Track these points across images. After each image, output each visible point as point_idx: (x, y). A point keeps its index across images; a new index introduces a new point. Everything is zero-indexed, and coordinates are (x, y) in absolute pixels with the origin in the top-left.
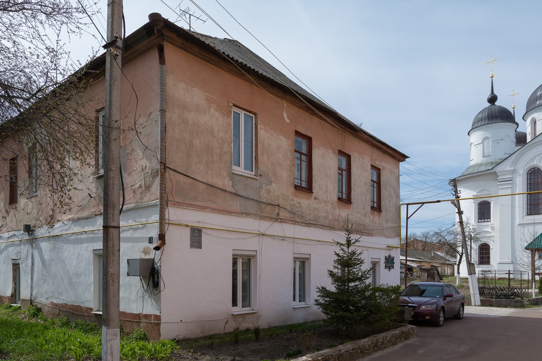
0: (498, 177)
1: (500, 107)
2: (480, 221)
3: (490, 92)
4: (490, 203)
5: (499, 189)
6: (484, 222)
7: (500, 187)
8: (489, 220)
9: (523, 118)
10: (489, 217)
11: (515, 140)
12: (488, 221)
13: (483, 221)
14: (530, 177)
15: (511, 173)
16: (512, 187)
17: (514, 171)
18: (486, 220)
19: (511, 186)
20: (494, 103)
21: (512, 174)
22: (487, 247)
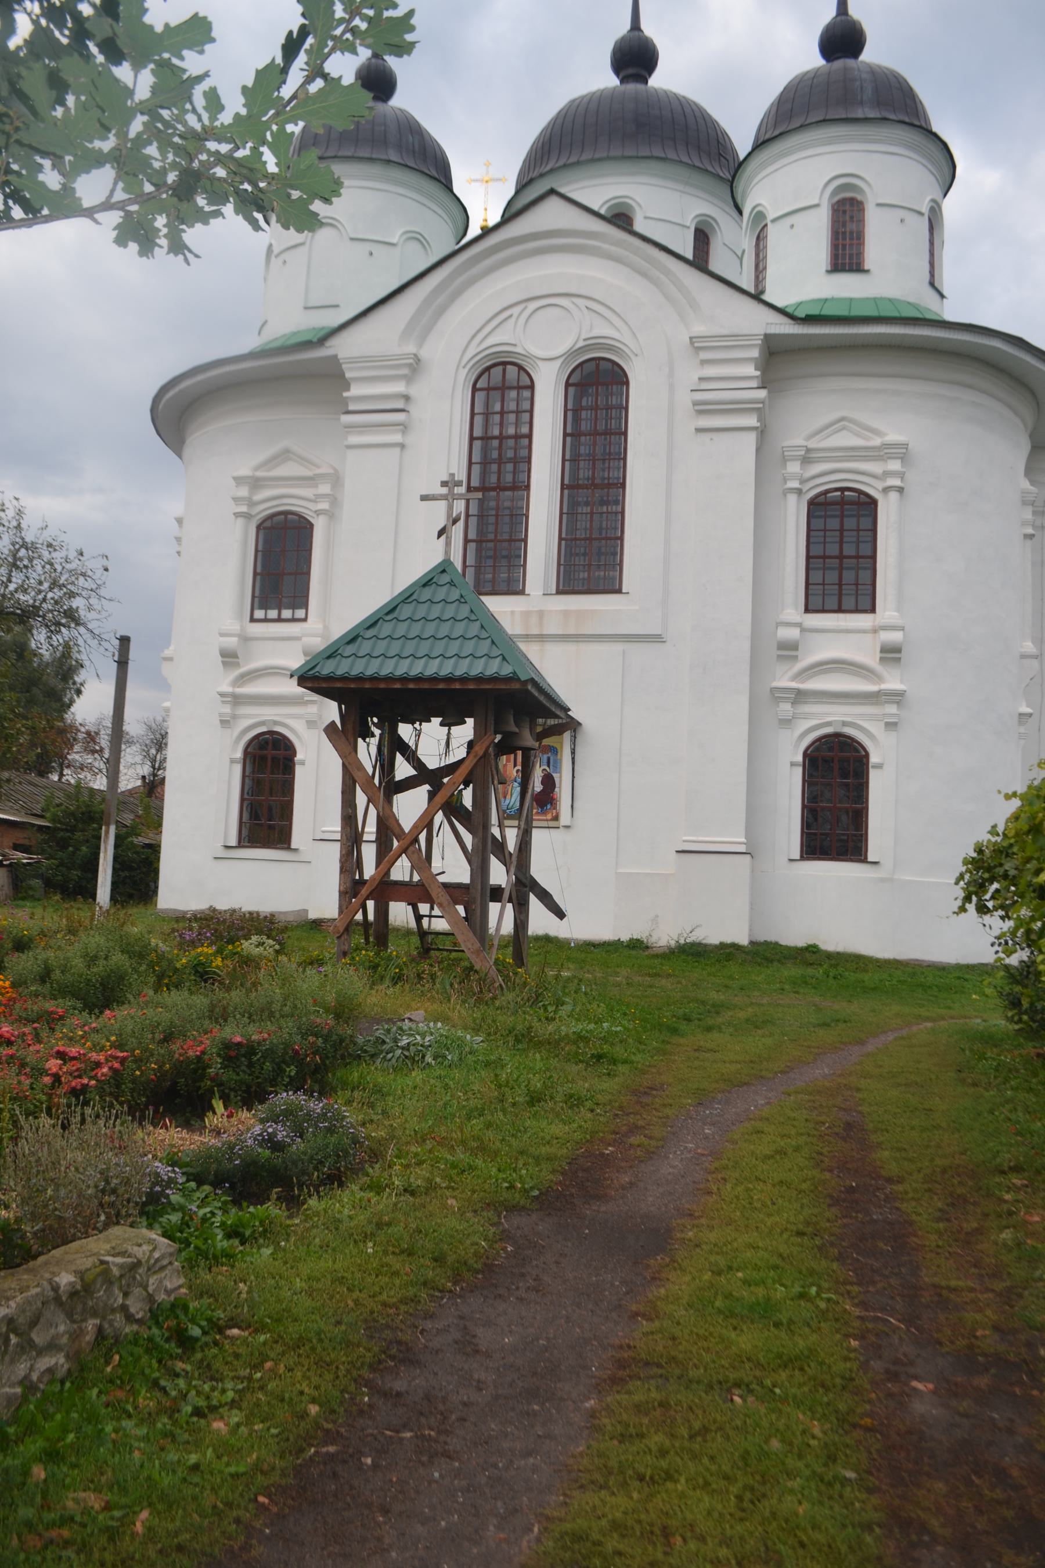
0: (346, 385)
2: (259, 614)
4: (311, 526)
5: (350, 447)
6: (279, 620)
7: (354, 439)
8: (300, 613)
10: (300, 599)
12: (294, 620)
13: (273, 614)
15: (405, 371)
16: (402, 446)
17: (415, 367)
18: (287, 613)
19: (397, 438)
21: (409, 379)
22: (280, 753)
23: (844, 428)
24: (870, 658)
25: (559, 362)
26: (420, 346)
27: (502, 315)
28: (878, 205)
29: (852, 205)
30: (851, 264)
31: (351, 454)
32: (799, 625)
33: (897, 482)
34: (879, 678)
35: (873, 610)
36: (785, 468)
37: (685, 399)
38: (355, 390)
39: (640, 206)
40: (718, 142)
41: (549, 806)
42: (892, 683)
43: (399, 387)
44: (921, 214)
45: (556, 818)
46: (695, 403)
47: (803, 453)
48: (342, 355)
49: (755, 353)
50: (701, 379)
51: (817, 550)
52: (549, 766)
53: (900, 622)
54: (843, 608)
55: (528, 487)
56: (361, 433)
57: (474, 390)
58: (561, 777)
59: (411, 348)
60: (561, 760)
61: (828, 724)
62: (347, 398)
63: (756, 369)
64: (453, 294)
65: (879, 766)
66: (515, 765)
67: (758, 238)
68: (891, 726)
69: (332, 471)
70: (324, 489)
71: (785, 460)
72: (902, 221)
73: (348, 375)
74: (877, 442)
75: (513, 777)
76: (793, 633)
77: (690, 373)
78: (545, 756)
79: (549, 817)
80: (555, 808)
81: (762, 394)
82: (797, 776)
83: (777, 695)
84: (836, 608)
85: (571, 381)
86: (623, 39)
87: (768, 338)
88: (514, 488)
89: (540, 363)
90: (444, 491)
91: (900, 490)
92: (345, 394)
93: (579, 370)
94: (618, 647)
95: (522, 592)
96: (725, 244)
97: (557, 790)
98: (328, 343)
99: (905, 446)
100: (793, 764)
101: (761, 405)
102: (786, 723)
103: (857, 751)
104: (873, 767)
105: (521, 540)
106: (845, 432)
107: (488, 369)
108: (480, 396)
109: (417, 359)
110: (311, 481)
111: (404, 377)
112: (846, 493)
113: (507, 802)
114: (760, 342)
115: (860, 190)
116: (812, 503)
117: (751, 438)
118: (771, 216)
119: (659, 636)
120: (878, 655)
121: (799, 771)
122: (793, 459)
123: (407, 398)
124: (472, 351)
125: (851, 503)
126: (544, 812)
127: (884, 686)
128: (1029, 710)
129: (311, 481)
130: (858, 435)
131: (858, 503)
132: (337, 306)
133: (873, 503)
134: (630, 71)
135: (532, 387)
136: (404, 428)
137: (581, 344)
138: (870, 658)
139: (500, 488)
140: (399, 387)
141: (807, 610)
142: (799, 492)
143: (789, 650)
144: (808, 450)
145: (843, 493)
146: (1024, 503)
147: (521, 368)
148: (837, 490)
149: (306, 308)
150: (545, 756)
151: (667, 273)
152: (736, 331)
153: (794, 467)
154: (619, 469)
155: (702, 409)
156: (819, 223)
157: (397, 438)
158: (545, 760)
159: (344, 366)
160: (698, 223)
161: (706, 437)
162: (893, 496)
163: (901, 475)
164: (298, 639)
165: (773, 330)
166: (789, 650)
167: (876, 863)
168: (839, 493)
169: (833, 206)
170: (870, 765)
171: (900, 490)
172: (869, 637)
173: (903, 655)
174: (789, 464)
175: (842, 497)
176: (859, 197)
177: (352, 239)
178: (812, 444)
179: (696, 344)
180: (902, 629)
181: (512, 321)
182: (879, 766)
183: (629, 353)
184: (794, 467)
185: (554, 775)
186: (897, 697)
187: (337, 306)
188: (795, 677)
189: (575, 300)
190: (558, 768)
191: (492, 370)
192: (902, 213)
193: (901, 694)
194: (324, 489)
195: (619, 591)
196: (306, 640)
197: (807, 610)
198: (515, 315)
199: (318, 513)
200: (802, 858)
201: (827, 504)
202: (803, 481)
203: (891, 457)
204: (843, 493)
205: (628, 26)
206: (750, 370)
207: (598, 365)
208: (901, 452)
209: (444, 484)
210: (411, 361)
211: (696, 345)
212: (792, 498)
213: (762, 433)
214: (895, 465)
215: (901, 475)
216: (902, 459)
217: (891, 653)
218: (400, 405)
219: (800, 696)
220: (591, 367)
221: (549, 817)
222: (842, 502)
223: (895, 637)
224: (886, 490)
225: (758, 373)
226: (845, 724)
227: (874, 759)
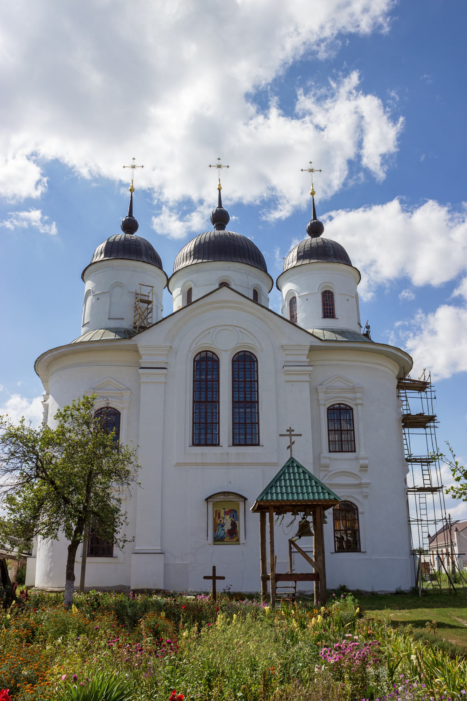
4: (120, 414)
24: (356, 470)
29: (329, 293)
30: (330, 316)
35: (355, 451)
41: (234, 535)
45: (238, 540)
47: (325, 390)
49: (307, 352)
50: (286, 361)
51: (332, 428)
52: (233, 518)
54: (344, 450)
55: (219, 402)
57: (194, 361)
58: (239, 523)
60: (239, 515)
65: (363, 513)
66: (219, 518)
68: (366, 497)
72: (348, 300)
73: (141, 352)
75: (218, 523)
76: (327, 461)
78: (232, 514)
79: (235, 540)
80: (237, 536)
81: (311, 368)
84: (341, 450)
87: (311, 346)
88: (212, 402)
90: (288, 433)
91: (362, 404)
92: (140, 360)
93: (237, 355)
95: (218, 445)
97: (238, 528)
101: (311, 373)
104: (360, 513)
107: (200, 353)
112: (341, 405)
113: (216, 534)
114: (309, 348)
116: (328, 409)
124: (194, 346)
125: (343, 409)
126: (232, 538)
127: (362, 481)
131: (346, 409)
133: (352, 409)
137: (238, 345)
138: (356, 470)
139: (206, 401)
141: (330, 452)
145: (340, 406)
147: (213, 353)
150: (232, 514)
158: (232, 516)
162: (360, 407)
165: (313, 344)
167: (365, 552)
168: (338, 405)
171: (362, 404)
176: (331, 290)
180: (367, 459)
185: (236, 522)
189: (235, 328)
190: (237, 518)
193: (368, 484)
195: (258, 445)
197: (330, 452)
200: (336, 552)
201: (333, 409)
204: (340, 406)
206: (304, 359)
207: (245, 354)
209: (288, 431)
211: (284, 348)
214: (359, 395)
220: (243, 353)
221: (235, 540)
222: (340, 409)
224: (356, 405)
226: (348, 496)
227: (360, 510)
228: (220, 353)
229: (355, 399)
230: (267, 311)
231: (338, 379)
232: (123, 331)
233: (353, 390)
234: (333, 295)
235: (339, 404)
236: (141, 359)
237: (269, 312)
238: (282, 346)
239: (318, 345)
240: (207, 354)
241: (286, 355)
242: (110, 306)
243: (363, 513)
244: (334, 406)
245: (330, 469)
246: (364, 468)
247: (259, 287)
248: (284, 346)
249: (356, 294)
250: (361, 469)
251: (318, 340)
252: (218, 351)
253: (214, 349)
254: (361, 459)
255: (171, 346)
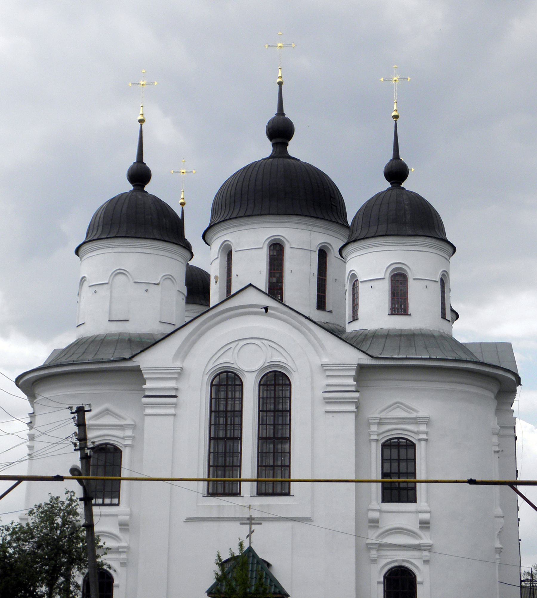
0: (144, 382)
1: (157, 201)
3: (134, 159)
7: (148, 411)
9: (204, 237)
11: (185, 290)
14: (218, 392)
15: (176, 376)
16: (174, 415)
17: (180, 374)
19: (172, 411)
20: (144, 187)
23: (398, 407)
24: (414, 526)
25: (255, 374)
26: (183, 361)
27: (226, 348)
28: (414, 279)
31: (147, 419)
32: (380, 511)
33: (424, 436)
34: (420, 537)
35: (415, 501)
36: (370, 428)
37: (319, 394)
38: (148, 385)
39: (288, 241)
40: (331, 197)
42: (426, 539)
43: (172, 384)
44: (437, 282)
46: (325, 398)
47: (378, 421)
48: (142, 366)
49: (353, 373)
50: (327, 385)
51: (387, 470)
53: (428, 509)
56: (152, 407)
57: (212, 385)
59: (178, 364)
61: (396, 561)
62: (145, 388)
63: (355, 380)
64: (199, 334)
67: (354, 285)
68: (426, 562)
69: (133, 423)
70: (129, 433)
71: (369, 424)
73: (145, 376)
74: (414, 415)
77: (322, 382)
81: (357, 395)
82: (381, 588)
83: (369, 547)
85: (261, 383)
86: (273, 119)
87: (358, 364)
89: (246, 373)
92: (144, 386)
94: (290, 524)
96: (335, 257)
98: (135, 359)
99: (429, 418)
100: (379, 583)
101: (357, 400)
102: (374, 561)
103: (411, 575)
104: (418, 583)
105: (237, 466)
106: (398, 409)
107: (219, 374)
108: (214, 388)
109: (182, 369)
110: (122, 427)
111: (176, 379)
114: (355, 368)
115: (405, 271)
116: (384, 445)
117: (353, 416)
118: (359, 280)
119: (310, 518)
120: (418, 525)
121: (382, 586)
122: (374, 424)
123: (177, 389)
124: (210, 366)
128: (501, 546)
129: (122, 427)
130: (405, 411)
132: (128, 320)
133: (413, 445)
134: (279, 140)
135: (241, 385)
136: (175, 405)
137: (267, 364)
138: (414, 526)
140: (172, 384)
142: (377, 440)
143: (374, 523)
144: (381, 419)
145: (398, 440)
146: (494, 434)
147: (236, 374)
148: (396, 438)
149: (109, 321)
151: (310, 330)
152: (344, 362)
153: (374, 428)
154: (286, 429)
155: (328, 401)
156: (385, 287)
157: (172, 411)
159: (143, 371)
160: (321, 247)
161: (330, 415)
162: (423, 443)
163: (427, 433)
164: (116, 515)
166: (374, 523)
168: (397, 440)
169: (391, 277)
170: (417, 582)
171: (426, 440)
172: (413, 515)
173: (431, 525)
174: (371, 435)
175: (399, 442)
177: (135, 282)
178: (383, 415)
179: (324, 367)
180: (430, 512)
181: (231, 350)
182: (422, 583)
183: (289, 368)
184: (374, 428)
186: (429, 548)
187: (128, 320)
188: (379, 536)
189: (263, 341)
191: (221, 375)
192: (427, 283)
194: (129, 433)
195: (288, 494)
196: (121, 518)
198: (233, 347)
199: (126, 446)
202: (378, 435)
203: (422, 423)
204: (398, 440)
205: (276, 111)
206: (351, 382)
208: (427, 421)
210: (179, 371)
211: (324, 368)
212: (374, 444)
213: (357, 413)
214: (423, 428)
215: (427, 433)
216: (426, 424)
217: (425, 525)
218: (173, 393)
219: (381, 547)
223: (426, 516)
224: (420, 440)
225: (355, 383)
227: (419, 579)
228: (243, 374)
229: (418, 433)
230: (304, 318)
231: (398, 404)
232: (127, 339)
233: (416, 421)
234: (407, 280)
235: (399, 438)
236: (145, 384)
237: (306, 319)
238: (322, 365)
239: (371, 363)
240: (227, 375)
241: (328, 376)
242: (111, 302)
243: (422, 583)
244: (392, 441)
245: (380, 525)
246: (425, 525)
247: (326, 244)
248: (323, 365)
249: (443, 275)
250: (428, 526)
251: (368, 356)
252: (241, 372)
253: (236, 370)
254: (421, 512)
255: (182, 369)
